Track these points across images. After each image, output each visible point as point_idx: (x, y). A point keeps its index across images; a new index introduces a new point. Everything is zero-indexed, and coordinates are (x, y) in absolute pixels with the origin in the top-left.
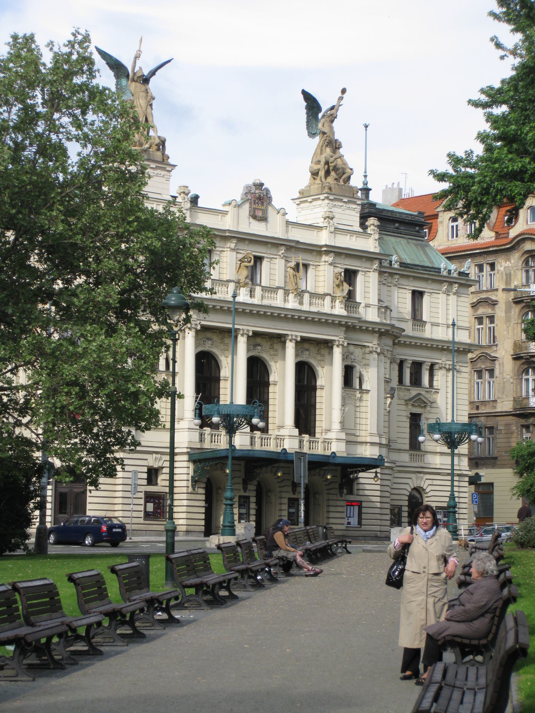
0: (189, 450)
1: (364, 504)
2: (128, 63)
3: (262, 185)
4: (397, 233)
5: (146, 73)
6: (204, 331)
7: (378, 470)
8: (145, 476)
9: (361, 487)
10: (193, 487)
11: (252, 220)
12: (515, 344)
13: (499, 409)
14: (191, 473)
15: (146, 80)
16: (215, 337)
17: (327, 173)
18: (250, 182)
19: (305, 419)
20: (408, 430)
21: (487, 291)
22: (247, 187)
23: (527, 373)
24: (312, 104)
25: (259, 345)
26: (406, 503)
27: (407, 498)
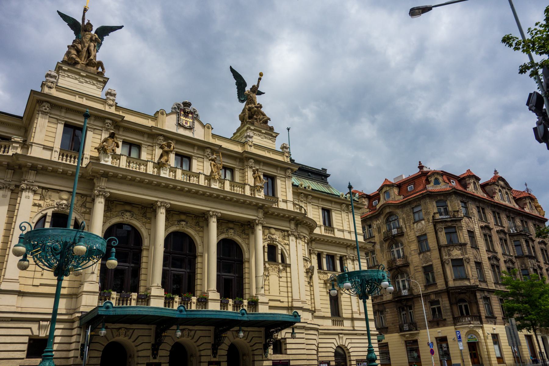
8: (25, 347)
11: (179, 127)
12: (388, 262)
16: (136, 211)
17: (250, 117)
18: (180, 102)
21: (369, 238)
24: (241, 83)
25: (183, 221)
26: (333, 359)
27: (333, 354)
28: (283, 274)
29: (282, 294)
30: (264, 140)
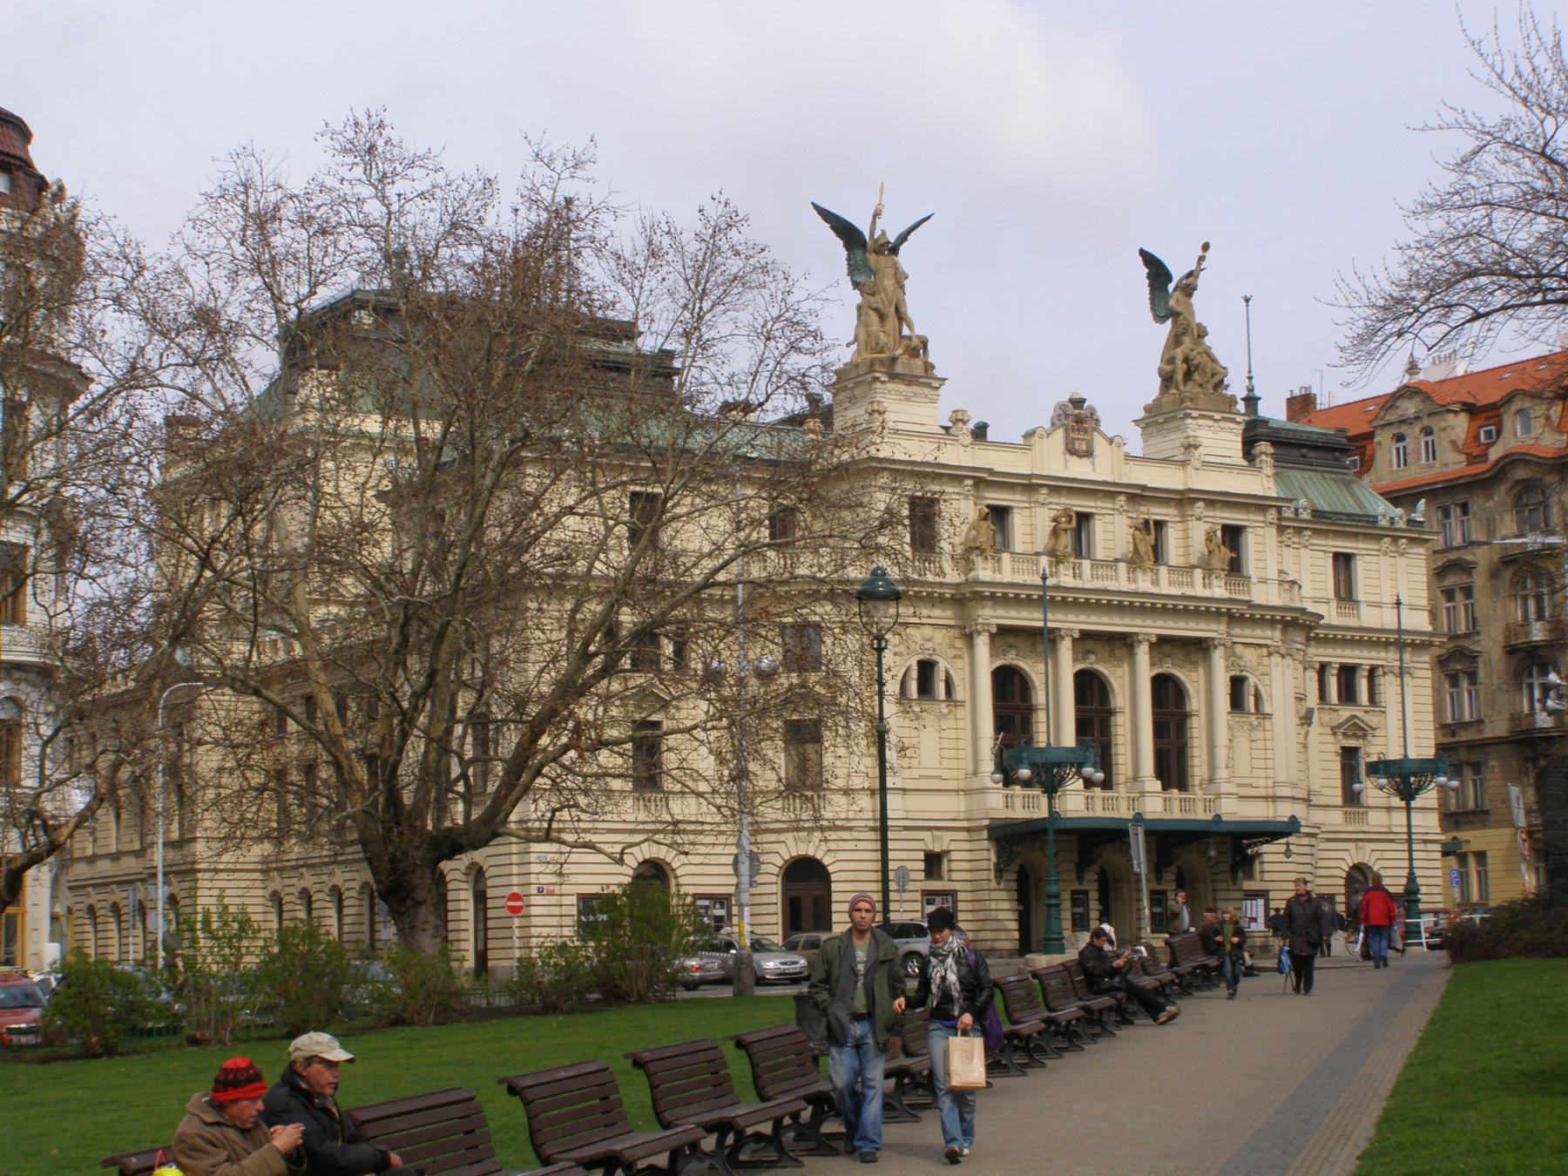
0: (986, 822)
1: (1272, 895)
2: (863, 226)
3: (1083, 401)
4: (1304, 464)
5: (892, 238)
6: (1005, 635)
7: (1291, 839)
8: (922, 865)
9: (1267, 867)
10: (999, 877)
12: (1508, 629)
13: (1487, 734)
14: (994, 858)
15: (894, 250)
17: (1188, 376)
19: (1172, 767)
20: (1338, 774)
22: (1061, 406)
23: (1530, 675)
24: (1157, 272)
25: (1092, 652)
26: (1343, 890)
28: (1259, 735)
29: (1256, 773)
30: (1221, 435)
